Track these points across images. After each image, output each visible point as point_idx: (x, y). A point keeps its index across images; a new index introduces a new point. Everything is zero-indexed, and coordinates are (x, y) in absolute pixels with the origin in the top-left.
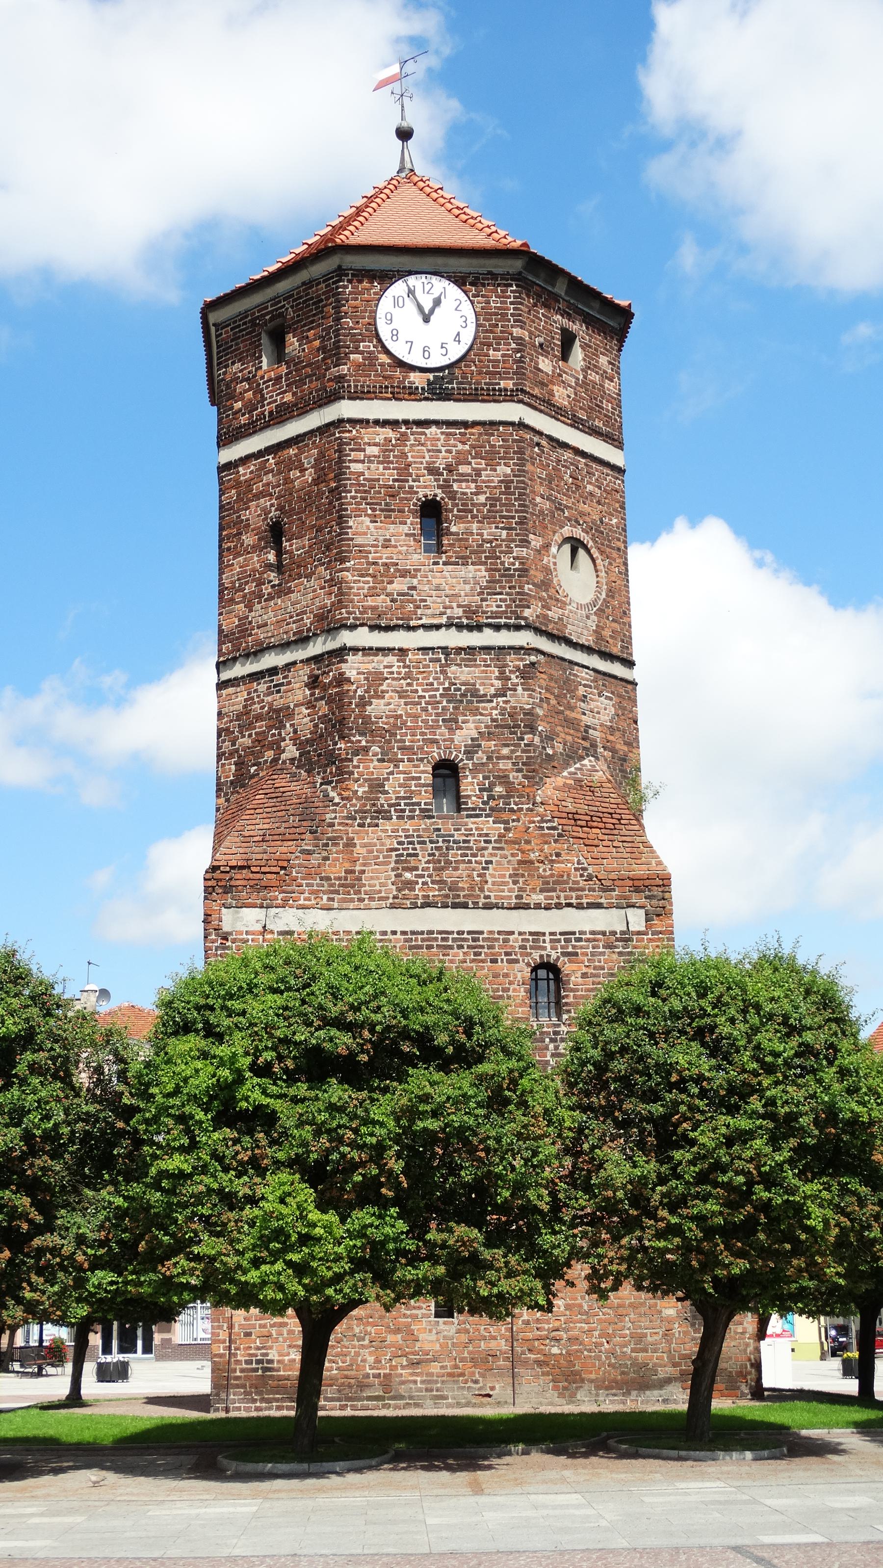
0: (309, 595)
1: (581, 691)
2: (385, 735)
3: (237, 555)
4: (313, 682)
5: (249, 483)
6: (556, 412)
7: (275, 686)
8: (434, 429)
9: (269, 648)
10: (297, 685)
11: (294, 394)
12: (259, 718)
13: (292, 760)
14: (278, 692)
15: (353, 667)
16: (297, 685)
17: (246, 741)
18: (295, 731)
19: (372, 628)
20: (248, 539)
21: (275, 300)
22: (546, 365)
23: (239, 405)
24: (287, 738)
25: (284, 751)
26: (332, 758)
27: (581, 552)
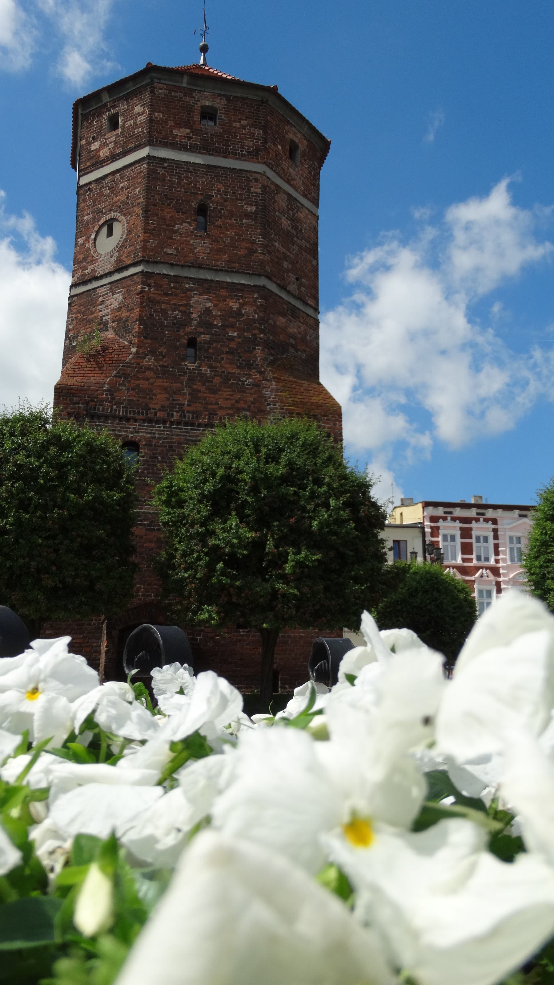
1: (101, 299)
6: (100, 164)
22: (95, 146)
27: (115, 224)
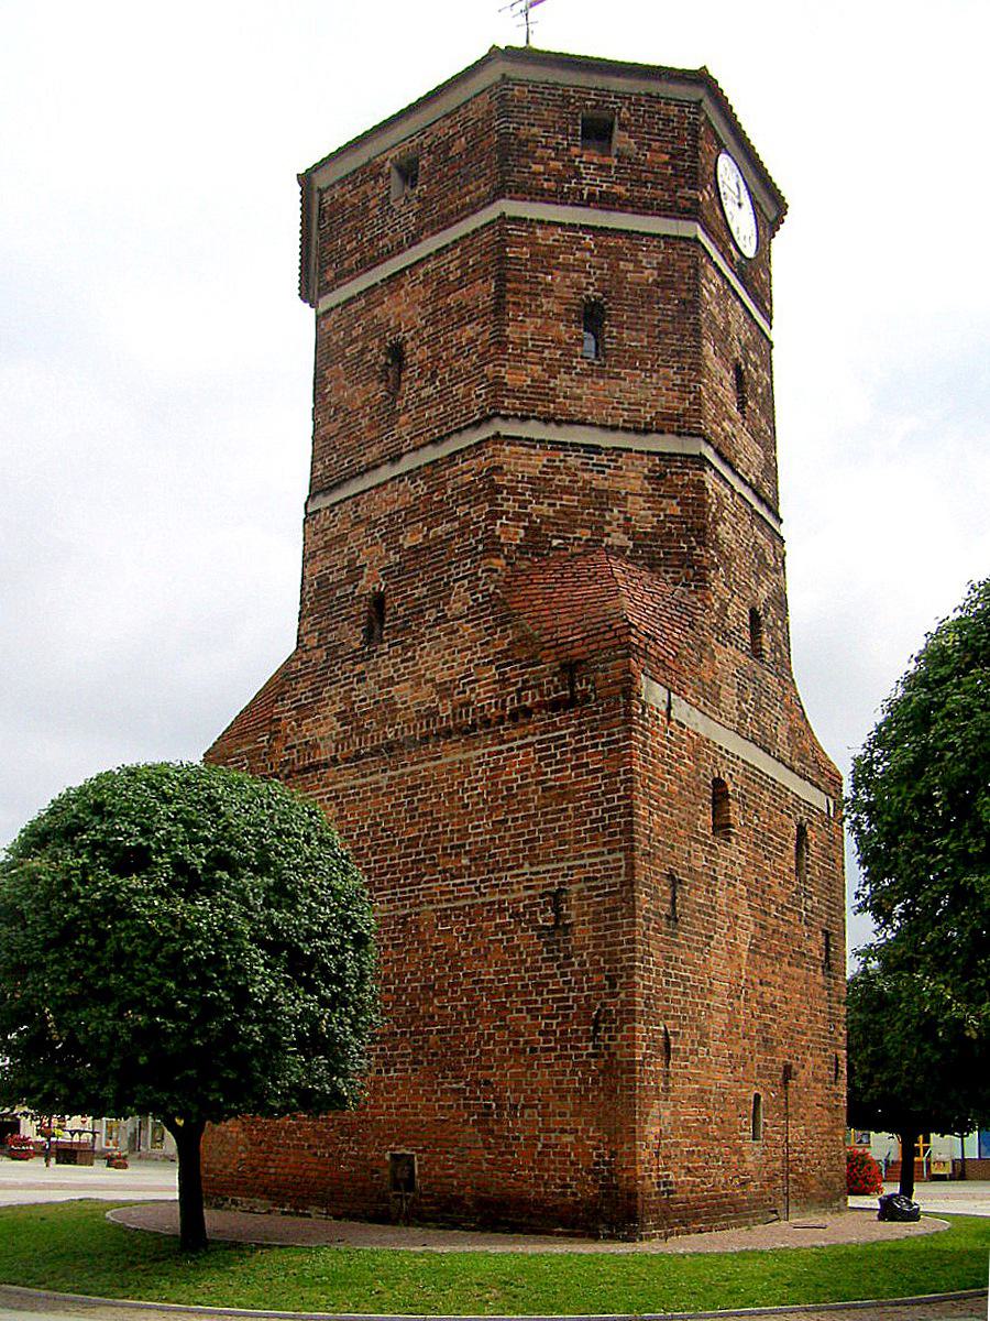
0: (648, 390)
2: (727, 559)
3: (533, 314)
4: (657, 478)
5: (552, 251)
7: (594, 465)
8: (738, 303)
9: (583, 423)
10: (633, 475)
11: (627, 190)
12: (567, 490)
13: (622, 549)
14: (603, 472)
15: (709, 477)
16: (633, 475)
17: (545, 509)
18: (628, 520)
19: (718, 452)
20: (548, 304)
21: (603, 92)
23: (541, 168)
24: (615, 523)
25: (608, 535)
26: (687, 561)
